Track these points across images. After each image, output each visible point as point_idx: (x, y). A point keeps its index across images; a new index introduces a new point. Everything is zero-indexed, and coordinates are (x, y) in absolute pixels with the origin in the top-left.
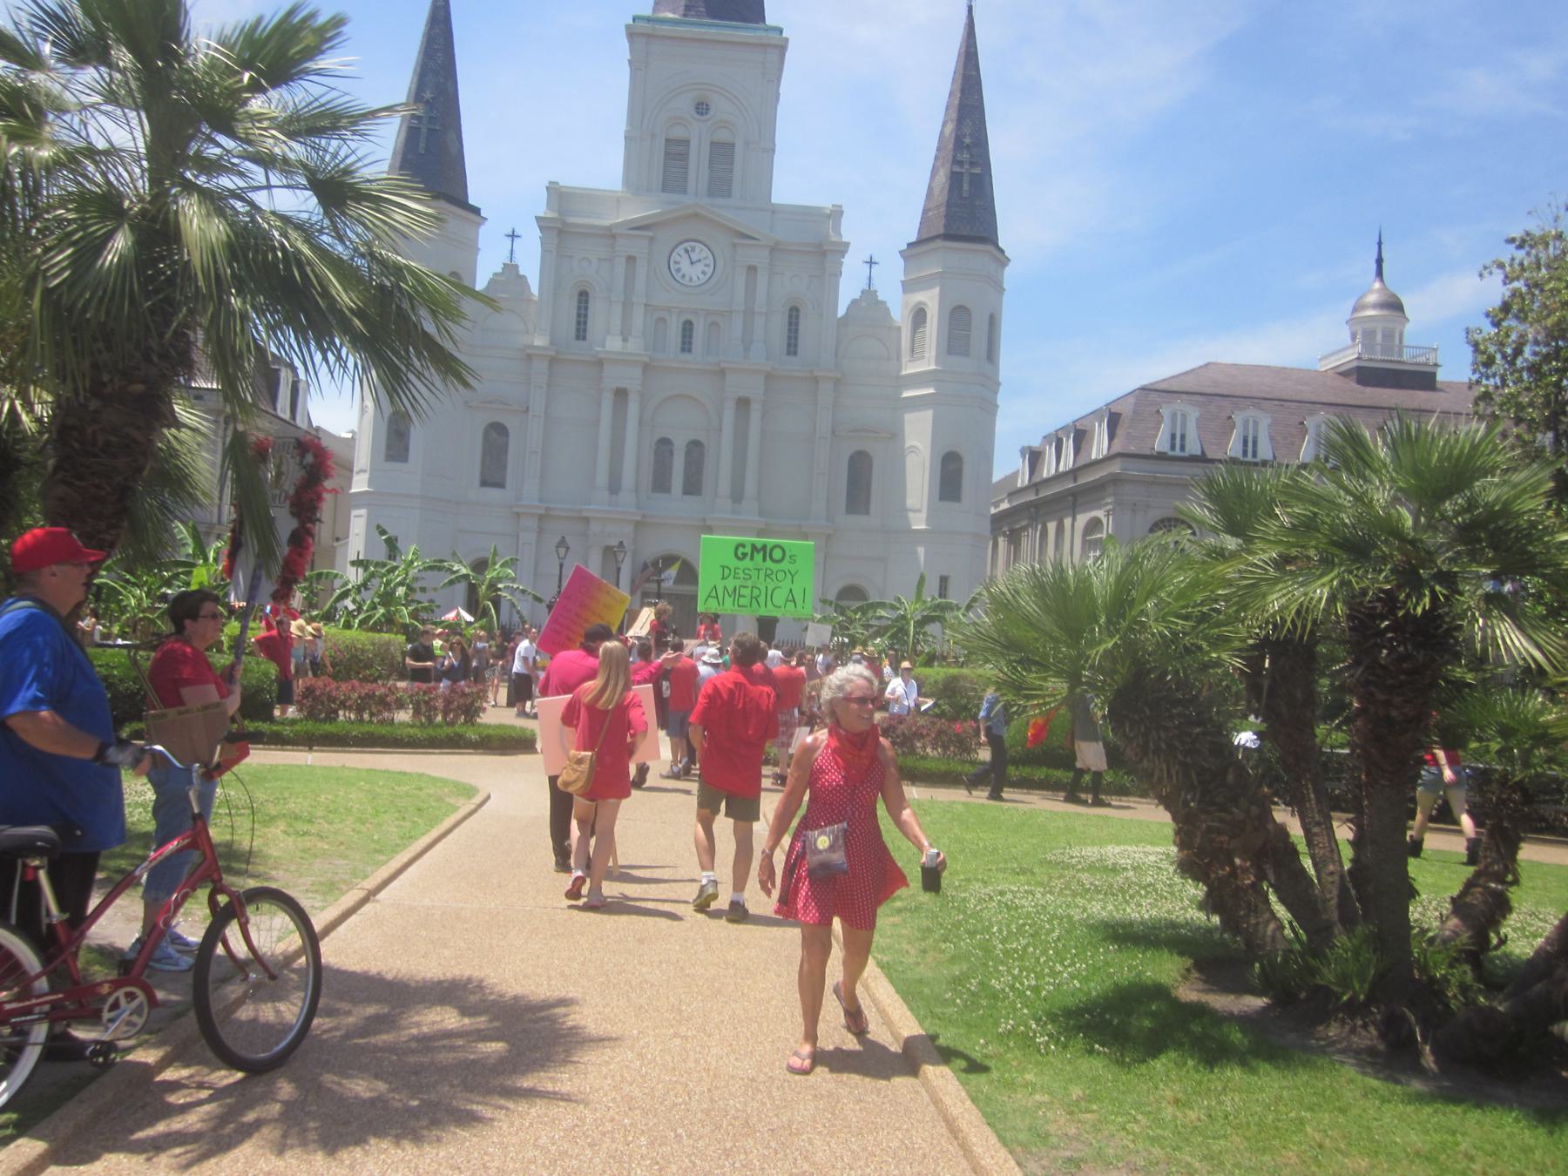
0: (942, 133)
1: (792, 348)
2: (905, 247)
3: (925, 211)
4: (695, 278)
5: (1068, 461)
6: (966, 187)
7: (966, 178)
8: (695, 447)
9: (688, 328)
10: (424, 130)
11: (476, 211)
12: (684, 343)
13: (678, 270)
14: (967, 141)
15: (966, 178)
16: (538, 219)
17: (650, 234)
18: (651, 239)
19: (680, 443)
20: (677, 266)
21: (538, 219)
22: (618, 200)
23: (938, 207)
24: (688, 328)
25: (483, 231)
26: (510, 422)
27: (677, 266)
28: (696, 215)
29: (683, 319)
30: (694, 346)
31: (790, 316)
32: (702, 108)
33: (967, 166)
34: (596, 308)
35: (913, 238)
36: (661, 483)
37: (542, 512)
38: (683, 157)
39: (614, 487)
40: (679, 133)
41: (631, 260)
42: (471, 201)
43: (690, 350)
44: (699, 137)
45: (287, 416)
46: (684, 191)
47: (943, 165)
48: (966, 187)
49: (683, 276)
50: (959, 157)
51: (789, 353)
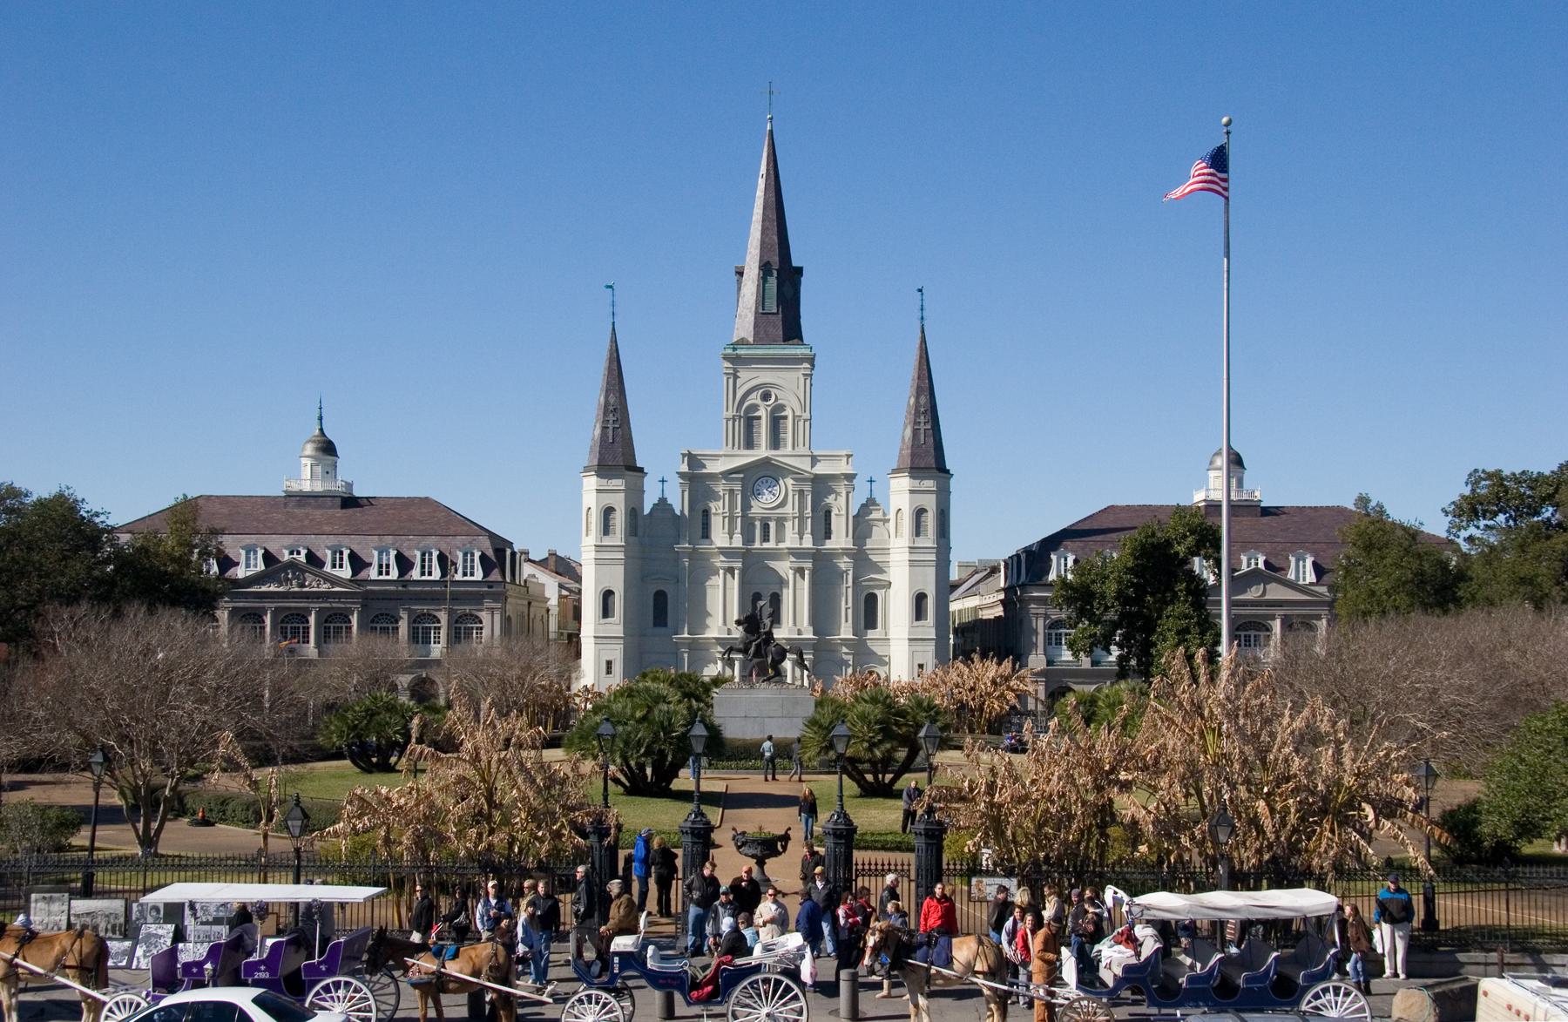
1: (828, 535)
3: (901, 450)
7: (922, 431)
10: (611, 428)
11: (641, 470)
17: (742, 476)
24: (766, 528)
26: (669, 590)
28: (766, 462)
32: (766, 397)
43: (768, 540)
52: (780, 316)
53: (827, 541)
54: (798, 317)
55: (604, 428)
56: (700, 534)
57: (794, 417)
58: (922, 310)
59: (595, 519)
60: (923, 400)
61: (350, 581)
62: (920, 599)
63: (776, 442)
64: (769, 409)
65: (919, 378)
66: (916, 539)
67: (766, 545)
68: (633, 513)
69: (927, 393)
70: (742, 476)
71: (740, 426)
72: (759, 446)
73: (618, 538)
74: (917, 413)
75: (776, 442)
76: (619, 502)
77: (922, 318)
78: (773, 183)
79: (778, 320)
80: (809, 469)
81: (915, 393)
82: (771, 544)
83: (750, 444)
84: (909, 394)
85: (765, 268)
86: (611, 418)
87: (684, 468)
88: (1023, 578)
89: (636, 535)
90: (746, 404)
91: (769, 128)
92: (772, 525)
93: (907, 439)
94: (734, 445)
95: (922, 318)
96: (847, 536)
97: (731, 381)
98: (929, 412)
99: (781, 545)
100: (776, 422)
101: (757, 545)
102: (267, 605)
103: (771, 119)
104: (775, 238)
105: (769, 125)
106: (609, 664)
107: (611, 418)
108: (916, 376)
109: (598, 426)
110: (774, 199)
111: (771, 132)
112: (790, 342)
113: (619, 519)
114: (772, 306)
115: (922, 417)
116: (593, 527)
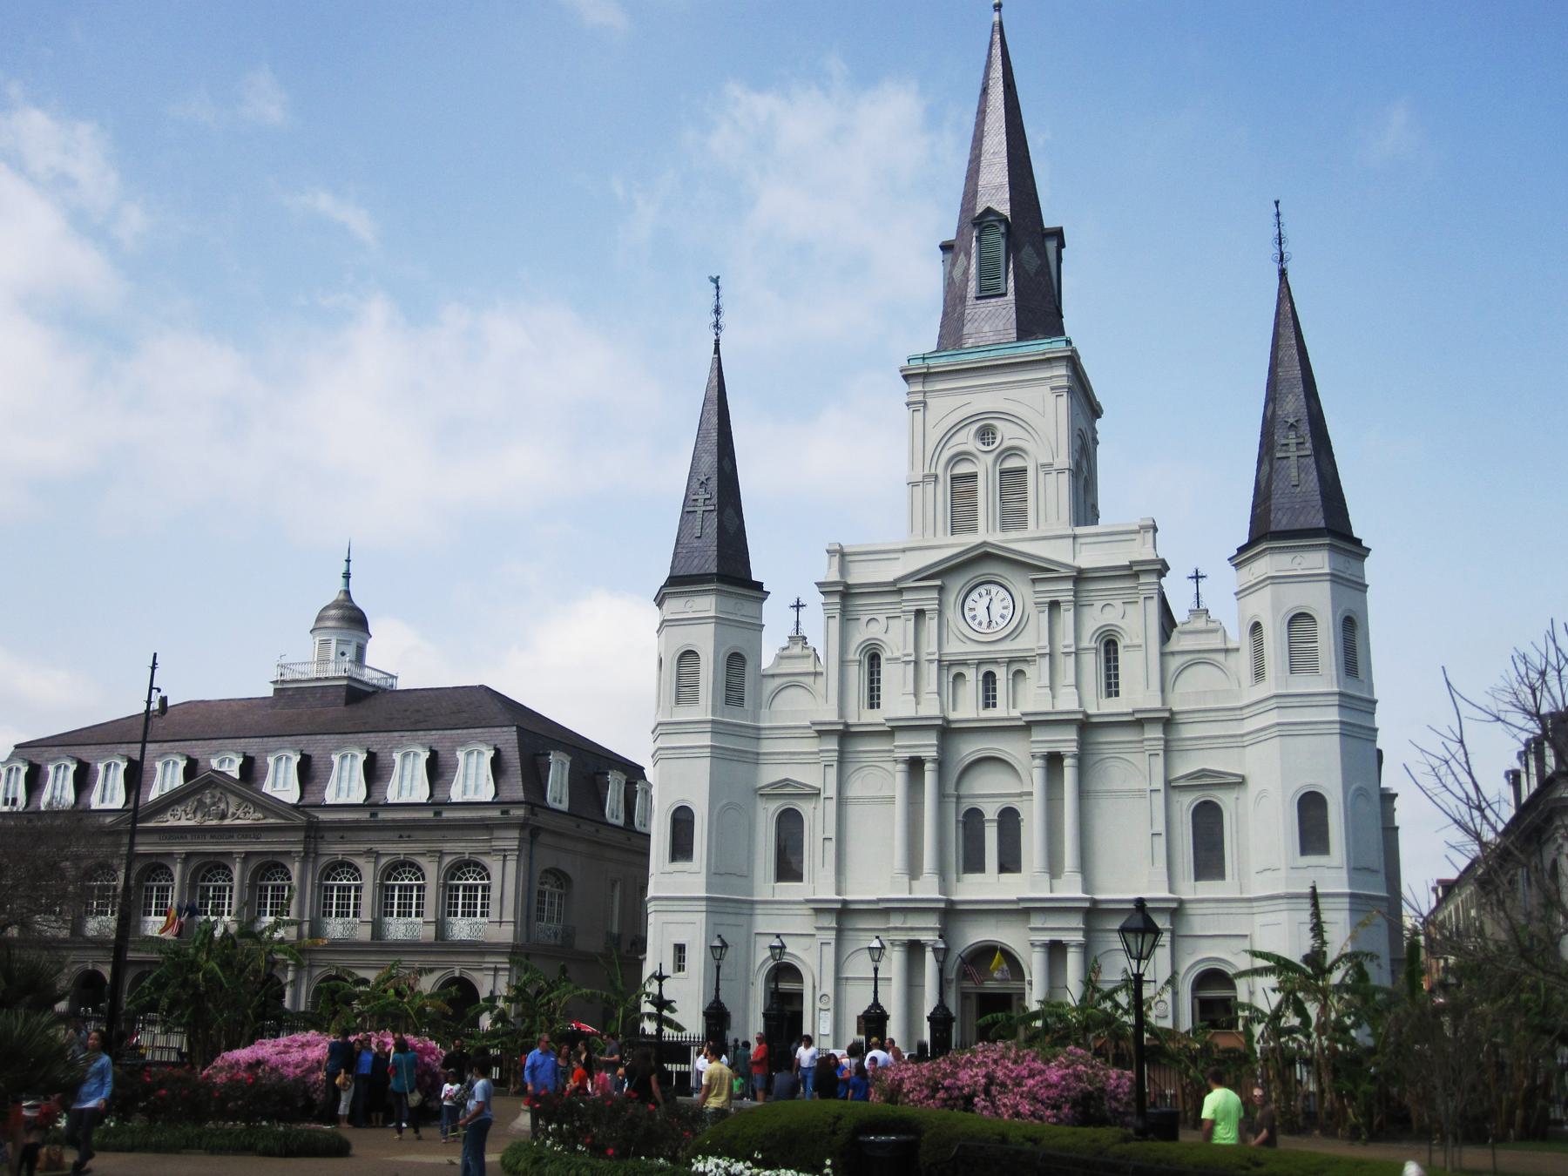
1: (1112, 688)
2: (1236, 552)
8: (1009, 820)
9: (989, 678)
10: (700, 510)
11: (758, 586)
13: (974, 618)
14: (1291, 420)
16: (818, 584)
17: (938, 582)
18: (941, 589)
19: (991, 811)
20: (973, 613)
21: (818, 584)
22: (904, 551)
24: (989, 678)
25: (767, 605)
26: (805, 808)
27: (973, 613)
29: (984, 669)
30: (1121, 689)
31: (1107, 652)
32: (986, 434)
34: (886, 668)
35: (1245, 540)
37: (839, 906)
39: (913, 869)
40: (964, 468)
41: (920, 614)
43: (994, 705)
44: (984, 467)
45: (621, 822)
46: (974, 529)
48: (1294, 472)
49: (980, 623)
50: (1284, 441)
51: (1109, 695)
61: (295, 807)
62: (1311, 807)
64: (991, 457)
68: (736, 663)
69: (1300, 389)
70: (938, 582)
72: (974, 529)
76: (704, 640)
77: (1282, 259)
80: (1069, 561)
82: (1000, 711)
86: (701, 497)
90: (947, 454)
91: (996, 17)
92: (1001, 674)
95: (1282, 259)
97: (919, 415)
98: (1305, 428)
99: (1015, 713)
102: (177, 849)
106: (680, 949)
112: (1034, 337)
113: (707, 672)
115: (1292, 434)
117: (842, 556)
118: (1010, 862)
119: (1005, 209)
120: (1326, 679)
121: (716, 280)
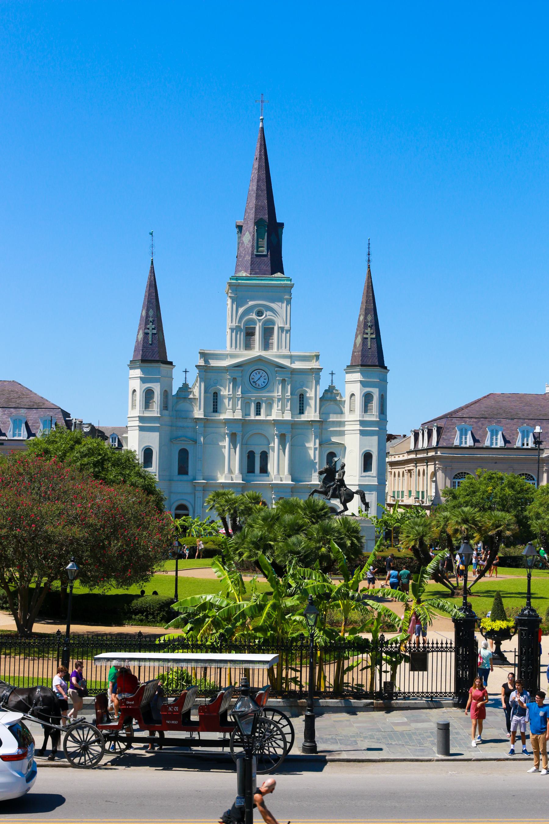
0: (359, 319)
2: (345, 367)
3: (353, 352)
4: (260, 385)
5: (425, 445)
6: (369, 343)
7: (369, 340)
8: (265, 456)
10: (150, 333)
11: (171, 363)
12: (257, 411)
14: (369, 324)
15: (369, 340)
23: (358, 352)
25: (174, 370)
28: (260, 360)
31: (300, 398)
32: (260, 314)
33: (369, 335)
36: (250, 469)
38: (253, 334)
42: (169, 359)
47: (360, 334)
48: (369, 343)
49: (256, 384)
52: (269, 257)
53: (302, 415)
54: (281, 257)
55: (146, 334)
56: (212, 410)
57: (279, 328)
58: (369, 254)
59: (139, 397)
60: (369, 318)
63: (266, 345)
65: (366, 303)
66: (365, 415)
67: (258, 418)
68: (166, 394)
71: (242, 336)
72: (254, 348)
73: (155, 411)
74: (366, 326)
75: (266, 345)
77: (369, 261)
78: (264, 164)
79: (267, 260)
81: (363, 313)
82: (262, 417)
83: (248, 346)
84: (358, 313)
85: (258, 223)
87: (202, 363)
88: (434, 443)
89: (167, 410)
91: (261, 125)
93: (358, 345)
94: (236, 347)
95: (369, 261)
96: (315, 411)
98: (374, 327)
100: (268, 332)
101: (253, 417)
103: (262, 119)
104: (266, 202)
105: (261, 123)
107: (150, 326)
108: (365, 301)
109: (141, 332)
110: (264, 175)
111: (262, 128)
114: (264, 250)
116: (138, 403)
117: (204, 355)
118: (264, 470)
119: (266, 217)
120: (373, 416)
121: (151, 234)
